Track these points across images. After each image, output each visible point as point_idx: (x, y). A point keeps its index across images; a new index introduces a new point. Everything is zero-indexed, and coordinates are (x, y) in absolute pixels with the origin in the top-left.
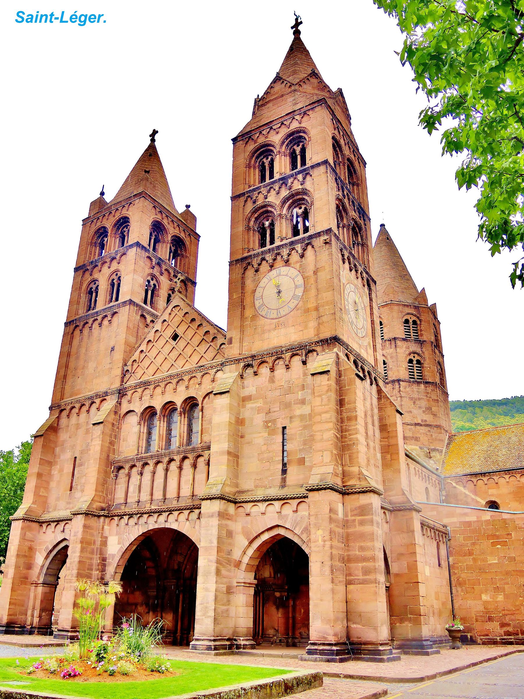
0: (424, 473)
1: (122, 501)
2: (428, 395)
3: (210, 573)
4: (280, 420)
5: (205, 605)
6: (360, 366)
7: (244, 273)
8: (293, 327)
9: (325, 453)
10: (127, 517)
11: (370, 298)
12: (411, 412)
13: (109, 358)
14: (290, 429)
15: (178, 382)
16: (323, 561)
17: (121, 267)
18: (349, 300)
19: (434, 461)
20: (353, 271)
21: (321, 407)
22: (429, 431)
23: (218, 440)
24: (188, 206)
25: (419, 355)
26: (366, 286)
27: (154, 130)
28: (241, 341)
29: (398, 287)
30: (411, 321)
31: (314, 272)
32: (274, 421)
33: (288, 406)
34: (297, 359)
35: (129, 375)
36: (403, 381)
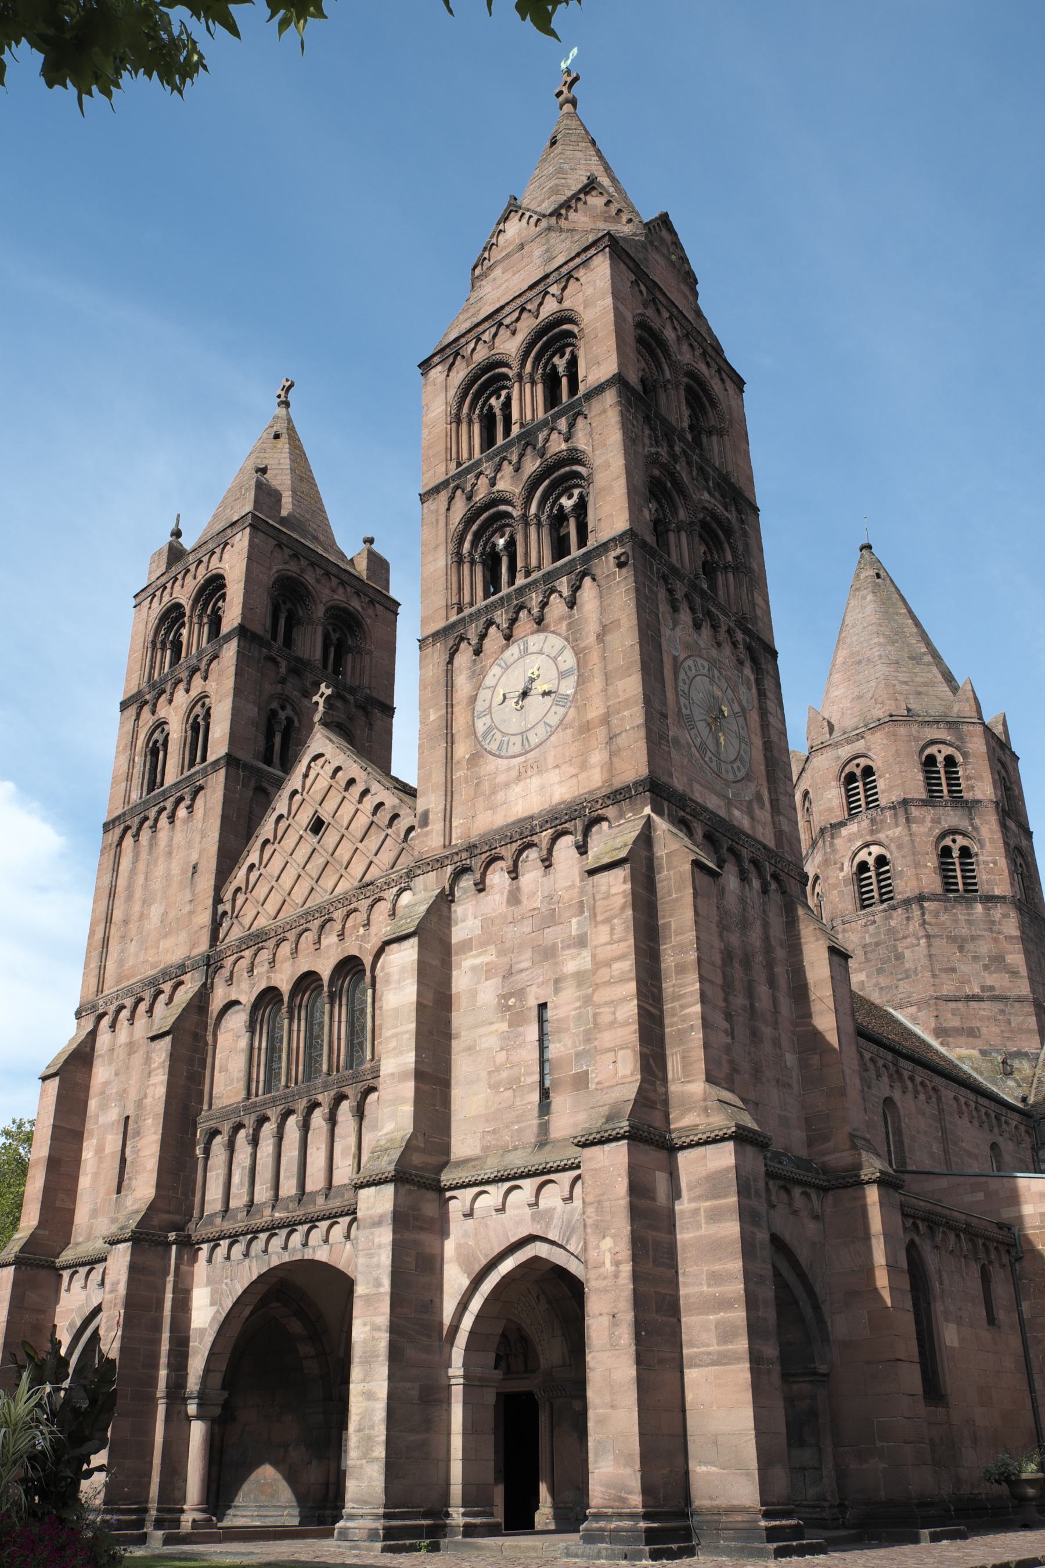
0: (983, 1110)
1: (218, 1207)
2: (995, 928)
3: (378, 1356)
4: (534, 988)
5: (367, 1432)
6: (725, 847)
7: (450, 662)
8: (557, 771)
9: (621, 1054)
10: (227, 1242)
11: (759, 690)
12: (953, 970)
13: (188, 890)
14: (555, 1007)
15: (322, 927)
16: (615, 1311)
17: (211, 687)
18: (693, 694)
19: (1016, 1081)
20: (706, 631)
21: (609, 947)
22: (1002, 1011)
23: (394, 1048)
24: (370, 541)
25: (964, 834)
26: (748, 664)
28: (448, 816)
29: (906, 683)
30: (940, 758)
31: (598, 636)
32: (520, 994)
34: (567, 841)
35: (229, 923)
36: (929, 900)
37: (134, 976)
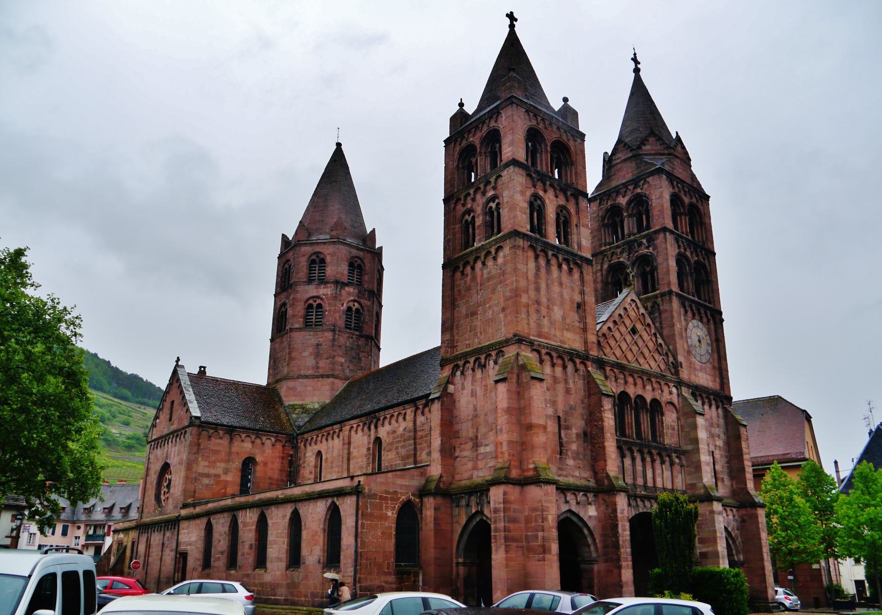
27: (507, 15)
37: (549, 339)
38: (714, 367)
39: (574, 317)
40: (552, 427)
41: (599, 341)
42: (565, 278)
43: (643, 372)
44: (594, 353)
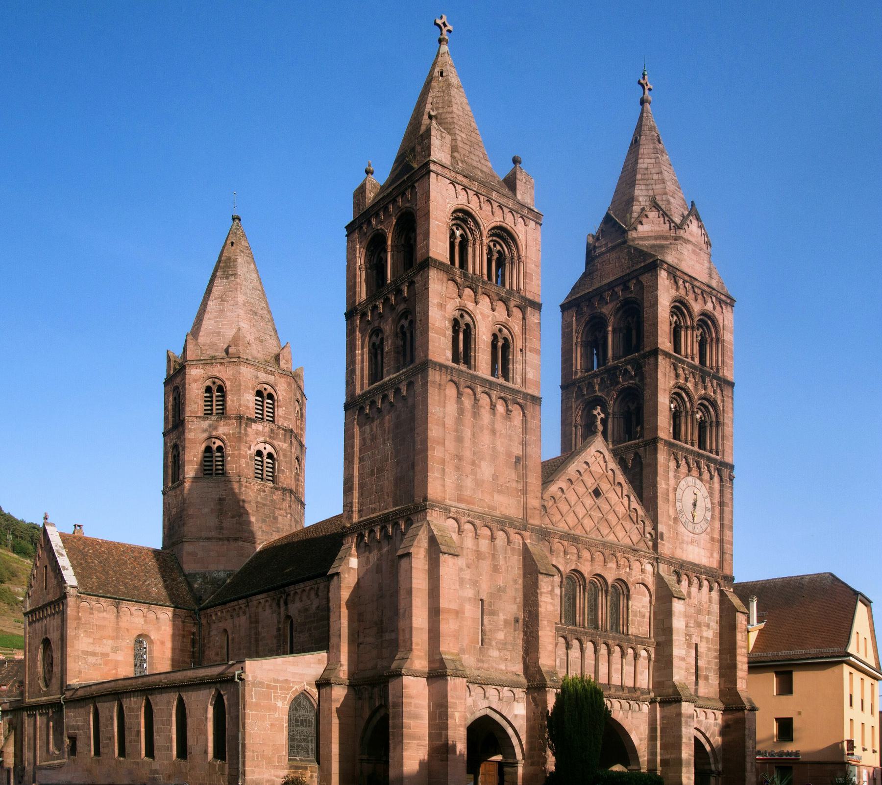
32: (690, 636)
33: (698, 625)
37: (473, 504)
38: (712, 539)
39: (509, 475)
40: (471, 611)
41: (544, 506)
42: (499, 425)
43: (605, 544)
44: (535, 521)
